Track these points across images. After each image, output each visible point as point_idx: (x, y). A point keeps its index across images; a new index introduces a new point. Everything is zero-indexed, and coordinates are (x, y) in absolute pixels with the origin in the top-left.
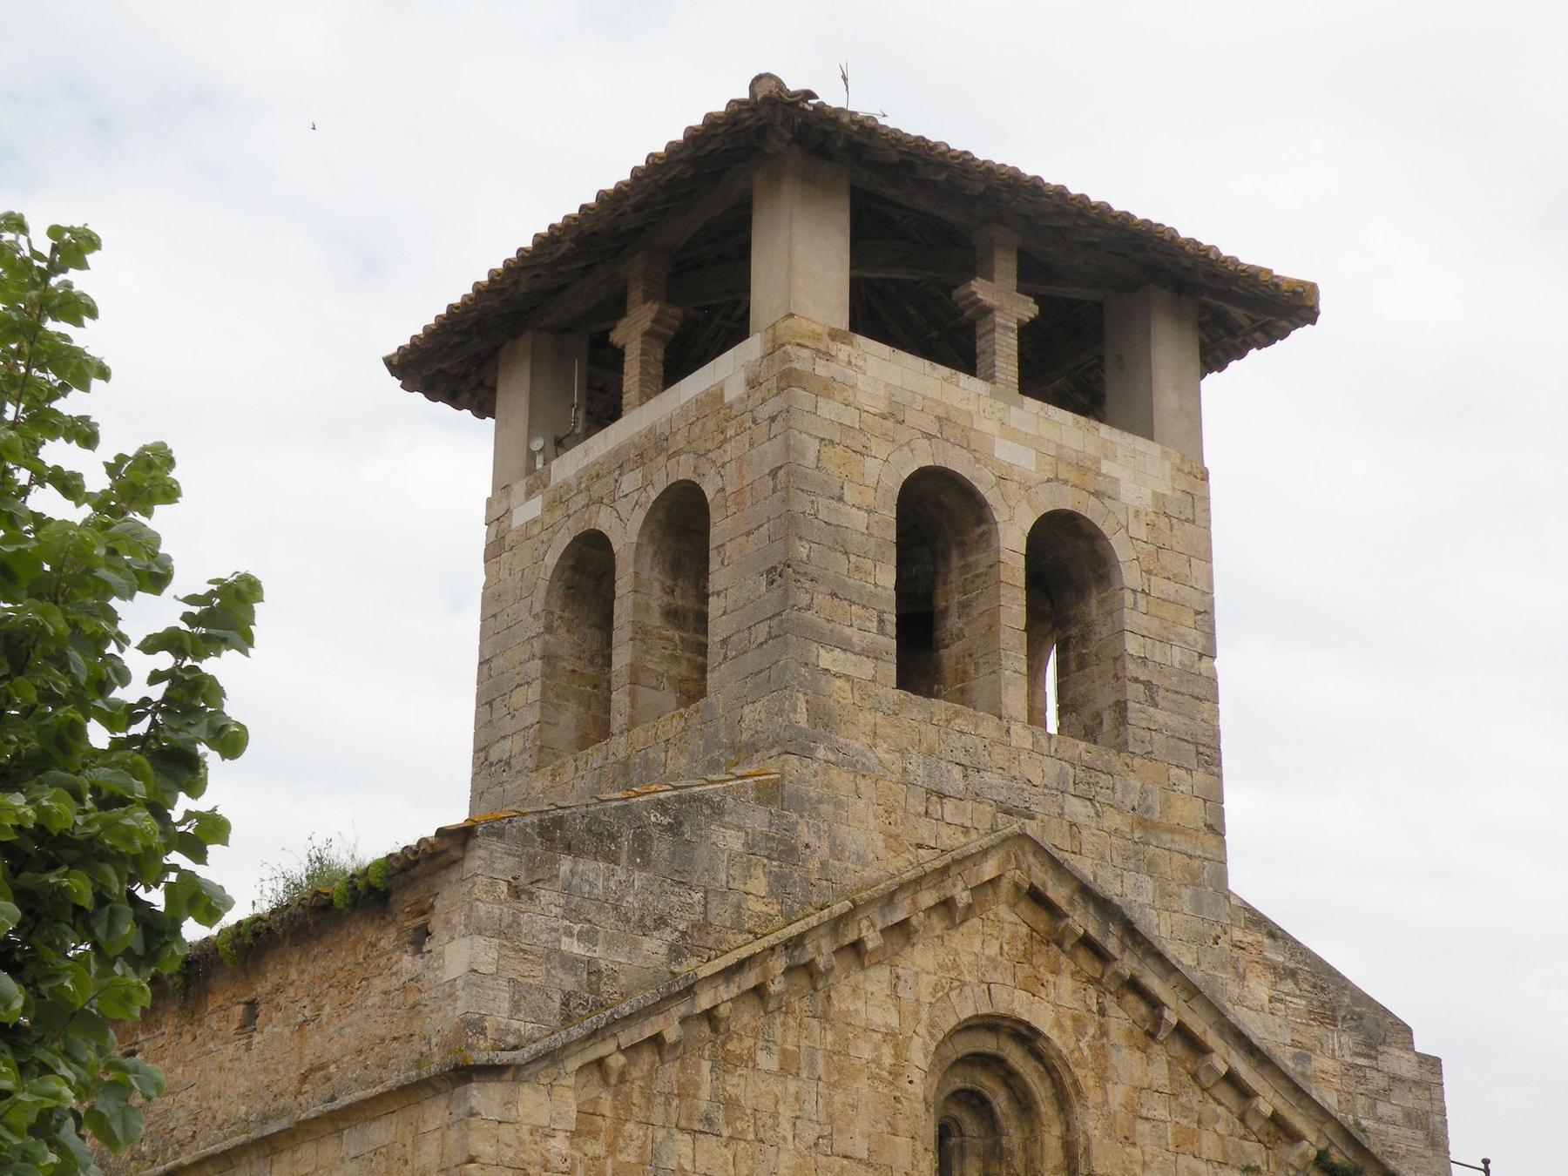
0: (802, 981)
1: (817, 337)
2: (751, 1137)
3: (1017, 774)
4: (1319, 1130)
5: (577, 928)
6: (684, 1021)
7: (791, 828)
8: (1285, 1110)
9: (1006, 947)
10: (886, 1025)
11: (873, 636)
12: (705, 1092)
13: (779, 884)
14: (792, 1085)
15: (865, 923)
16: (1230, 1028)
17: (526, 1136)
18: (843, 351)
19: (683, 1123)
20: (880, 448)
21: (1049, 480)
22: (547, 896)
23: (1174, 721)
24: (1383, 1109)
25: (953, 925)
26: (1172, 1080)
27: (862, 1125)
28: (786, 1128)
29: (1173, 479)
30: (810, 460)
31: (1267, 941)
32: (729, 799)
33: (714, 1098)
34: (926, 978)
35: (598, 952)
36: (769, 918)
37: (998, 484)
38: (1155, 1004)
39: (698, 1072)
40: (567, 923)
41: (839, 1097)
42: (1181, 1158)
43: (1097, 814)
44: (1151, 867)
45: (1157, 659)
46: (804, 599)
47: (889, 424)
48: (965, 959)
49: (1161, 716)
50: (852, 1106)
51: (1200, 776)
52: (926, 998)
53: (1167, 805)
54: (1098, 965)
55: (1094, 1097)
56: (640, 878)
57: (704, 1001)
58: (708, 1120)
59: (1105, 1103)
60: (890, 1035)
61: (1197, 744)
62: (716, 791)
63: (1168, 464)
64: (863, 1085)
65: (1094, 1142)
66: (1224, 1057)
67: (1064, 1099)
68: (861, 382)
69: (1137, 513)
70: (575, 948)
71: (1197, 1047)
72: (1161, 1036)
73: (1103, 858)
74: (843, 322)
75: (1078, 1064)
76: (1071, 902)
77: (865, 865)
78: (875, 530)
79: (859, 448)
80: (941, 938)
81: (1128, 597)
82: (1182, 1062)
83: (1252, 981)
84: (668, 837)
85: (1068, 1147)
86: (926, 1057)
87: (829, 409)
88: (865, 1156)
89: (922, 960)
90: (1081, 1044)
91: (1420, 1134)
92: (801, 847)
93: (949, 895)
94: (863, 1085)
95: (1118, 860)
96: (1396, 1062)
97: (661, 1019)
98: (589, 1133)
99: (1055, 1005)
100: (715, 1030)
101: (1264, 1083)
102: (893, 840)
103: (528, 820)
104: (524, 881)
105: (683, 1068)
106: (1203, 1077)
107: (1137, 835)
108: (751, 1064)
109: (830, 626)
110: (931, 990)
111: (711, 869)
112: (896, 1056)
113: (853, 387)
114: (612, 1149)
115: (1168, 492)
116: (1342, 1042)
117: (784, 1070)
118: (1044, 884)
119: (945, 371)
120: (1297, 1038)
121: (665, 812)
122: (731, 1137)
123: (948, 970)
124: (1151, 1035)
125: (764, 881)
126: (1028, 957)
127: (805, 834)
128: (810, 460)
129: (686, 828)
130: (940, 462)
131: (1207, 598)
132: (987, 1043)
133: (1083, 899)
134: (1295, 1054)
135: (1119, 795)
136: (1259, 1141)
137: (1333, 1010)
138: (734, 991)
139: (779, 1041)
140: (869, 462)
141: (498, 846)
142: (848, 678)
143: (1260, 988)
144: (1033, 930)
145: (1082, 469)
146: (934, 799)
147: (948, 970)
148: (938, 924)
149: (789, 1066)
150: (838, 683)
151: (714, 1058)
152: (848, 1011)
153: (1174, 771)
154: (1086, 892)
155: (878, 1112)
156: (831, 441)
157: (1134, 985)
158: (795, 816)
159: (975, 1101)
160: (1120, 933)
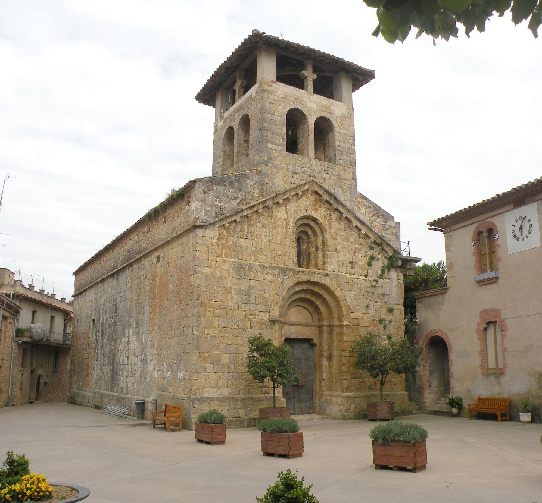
0: (266, 210)
1: (269, 82)
5: (218, 200)
6: (241, 217)
7: (264, 180)
8: (367, 233)
10: (284, 218)
11: (281, 142)
12: (246, 231)
13: (261, 191)
14: (264, 229)
15: (279, 198)
17: (208, 239)
18: (274, 85)
19: (241, 237)
20: (283, 104)
21: (319, 110)
22: (211, 193)
23: (346, 158)
24: (387, 232)
25: (299, 199)
26: (345, 228)
28: (263, 238)
29: (346, 110)
30: (267, 107)
31: (365, 201)
32: (250, 174)
33: (248, 232)
35: (222, 204)
36: (259, 197)
37: (308, 111)
38: (341, 213)
39: (244, 226)
40: (216, 199)
43: (329, 176)
44: (341, 187)
45: (343, 146)
46: (266, 134)
47: (285, 99)
48: (301, 205)
49: (343, 157)
50: (277, 233)
51: (351, 169)
52: (293, 213)
53: (344, 175)
54: (329, 206)
55: (328, 231)
56: (231, 190)
57: (245, 214)
58: (247, 236)
59: (331, 232)
60: (285, 220)
61: (351, 163)
62: (247, 173)
63: (345, 107)
64: (280, 229)
65: (328, 239)
66: (355, 223)
67: (322, 232)
68: (278, 91)
69: (338, 117)
70: (218, 204)
71: (350, 221)
72: (342, 219)
73: (330, 185)
74: (275, 80)
75: (325, 225)
76: (323, 194)
77: (279, 187)
78: (281, 120)
79: (278, 104)
80: (296, 201)
81: (336, 134)
82: (347, 224)
83: (361, 209)
84: (237, 182)
85: (323, 241)
86: (293, 224)
87: (271, 97)
89: (292, 206)
91: (395, 237)
92: (266, 184)
94: (280, 229)
95: (333, 185)
96: (391, 223)
98: (222, 239)
99: (320, 214)
100: (248, 219)
102: (285, 182)
103: (207, 179)
104: (206, 191)
105: (241, 226)
107: (338, 181)
109: (272, 140)
111: (246, 188)
112: (286, 224)
113: (277, 92)
114: (227, 241)
115: (345, 113)
116: (380, 220)
118: (318, 190)
119: (297, 89)
120: (370, 219)
121: (236, 177)
122: (252, 239)
124: (340, 219)
125: (258, 190)
126: (315, 204)
127: (266, 181)
128: (267, 107)
129: (241, 180)
130: (296, 107)
131: (353, 134)
132: (307, 222)
134: (370, 222)
135: (334, 173)
137: (378, 214)
138: (251, 211)
140: (280, 107)
141: (201, 184)
142: (276, 150)
143: (363, 210)
145: (326, 108)
146: (294, 174)
148: (295, 198)
149: (264, 226)
150: (274, 151)
151: (248, 224)
153: (346, 168)
154: (326, 192)
155: (282, 234)
156: (272, 103)
157: (337, 210)
158: (264, 177)
159: (305, 233)
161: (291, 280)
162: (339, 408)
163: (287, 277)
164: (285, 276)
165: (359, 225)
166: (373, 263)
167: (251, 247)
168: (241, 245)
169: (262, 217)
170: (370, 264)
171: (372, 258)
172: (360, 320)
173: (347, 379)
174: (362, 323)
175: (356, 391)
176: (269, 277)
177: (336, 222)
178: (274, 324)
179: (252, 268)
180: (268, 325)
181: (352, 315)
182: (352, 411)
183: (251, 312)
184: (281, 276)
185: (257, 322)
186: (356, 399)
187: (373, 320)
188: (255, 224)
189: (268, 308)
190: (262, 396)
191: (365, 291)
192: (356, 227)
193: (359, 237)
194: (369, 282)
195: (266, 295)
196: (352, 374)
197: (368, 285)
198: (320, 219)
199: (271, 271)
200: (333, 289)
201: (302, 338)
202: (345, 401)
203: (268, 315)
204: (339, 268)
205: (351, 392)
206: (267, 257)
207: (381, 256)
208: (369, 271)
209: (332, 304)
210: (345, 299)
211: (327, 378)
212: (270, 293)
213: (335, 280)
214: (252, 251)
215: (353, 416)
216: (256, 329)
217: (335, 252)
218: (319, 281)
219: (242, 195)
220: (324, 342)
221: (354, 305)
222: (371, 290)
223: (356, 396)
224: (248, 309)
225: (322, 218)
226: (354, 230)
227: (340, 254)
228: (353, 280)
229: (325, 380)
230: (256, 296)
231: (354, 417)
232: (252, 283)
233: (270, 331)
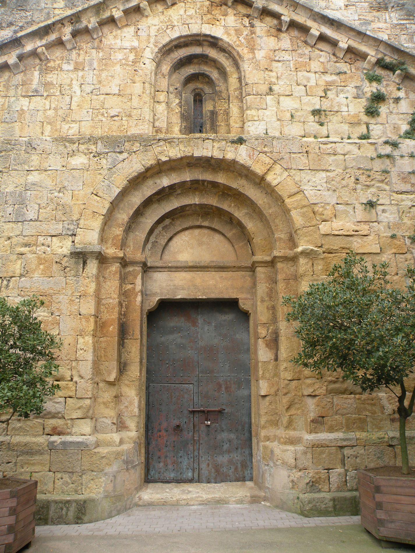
2: (58, 93)
4: (377, 50)
9: (197, 11)
12: (36, 81)
14: (80, 73)
15: (114, 10)
16: (317, 15)
19: (24, 94)
26: (292, 45)
27: (117, 81)
28: (76, 88)
34: (154, 27)
38: (277, 16)
39: (33, 75)
41: (104, 75)
42: (299, 73)
50: (112, 76)
52: (153, 32)
57: (29, 47)
58: (36, 91)
60: (133, 49)
64: (118, 68)
65: (247, 72)
66: (316, 29)
71: (304, 30)
72: (284, 28)
75: (238, 46)
86: (152, 54)
88: (117, 92)
90: (240, 39)
97: (6, 57)
99: (224, 26)
101: (342, 36)
106: (309, 41)
108: (59, 69)
110: (156, 30)
112: (136, 56)
117: (76, 69)
122: (48, 96)
123: (166, 23)
124: (279, 30)
136: (346, 62)
138: (44, 42)
139: (74, 59)
144: (212, 2)
147: (166, 23)
151: (40, 70)
152: (111, 44)
155: (124, 76)
161: (134, 160)
162: (289, 476)
163: (125, 155)
164: (121, 152)
165: (329, 32)
166: (383, 109)
167: (45, 110)
168: (22, 110)
169: (74, 52)
170: (371, 112)
171: (379, 98)
172: (351, 239)
173: (315, 396)
174: (357, 245)
175: (349, 427)
176: (79, 161)
178: (85, 263)
179: (36, 146)
180: (67, 264)
181: (324, 228)
182: (334, 487)
183: (26, 238)
184: (109, 154)
185: (39, 258)
186: (347, 452)
187: (393, 237)
188: (59, 67)
189: (69, 227)
190: (42, 440)
191: (359, 169)
192: (322, 38)
193: (335, 60)
194: (373, 148)
195: (66, 198)
196: (335, 382)
197: (369, 155)
198: (225, 38)
199: (82, 147)
200: (259, 169)
201: (204, 297)
202: (309, 456)
203: (70, 243)
204: (282, 125)
205: (331, 430)
206: (83, 123)
207: (406, 92)
208: (371, 128)
209: (270, 208)
210: (296, 190)
211: (272, 391)
212: (76, 192)
213: (266, 149)
214: (46, 117)
215: (331, 504)
216: (36, 275)
217: (267, 94)
218: (217, 154)
219: (27, 17)
220: (259, 303)
221: (328, 204)
222: (378, 165)
223: (345, 443)
224: (19, 233)
225: (229, 34)
226: (318, 46)
227: (282, 98)
228: (321, 146)
229: (268, 398)
230: (39, 202)
231: (334, 507)
232: (33, 177)
233: (71, 280)
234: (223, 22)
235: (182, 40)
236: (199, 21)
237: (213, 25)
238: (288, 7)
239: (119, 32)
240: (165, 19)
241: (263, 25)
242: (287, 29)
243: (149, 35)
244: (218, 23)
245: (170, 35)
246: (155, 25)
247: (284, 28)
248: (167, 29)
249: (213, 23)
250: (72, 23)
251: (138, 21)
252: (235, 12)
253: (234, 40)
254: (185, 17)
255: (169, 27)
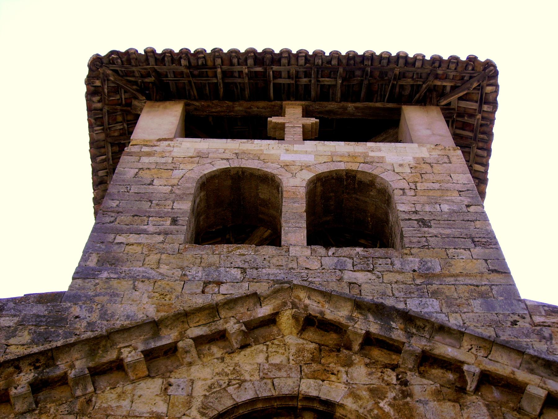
3: (295, 266)
9: (291, 358)
16: (536, 362)
49: (433, 231)
52: (199, 390)
72: (471, 385)
90: (381, 405)
93: (221, 328)
99: (347, 383)
110: (207, 387)
118: (322, 313)
123: (227, 375)
133: (361, 313)
160: (402, 326)
177: (439, 400)
234: (344, 376)
235: (260, 406)
236: (295, 375)
237: (323, 381)
238: (473, 350)
239: (129, 387)
240: (226, 370)
241: (425, 381)
242: (477, 389)
243: (190, 395)
244: (333, 378)
245: (234, 396)
246: (205, 380)
247: (471, 385)
248: (229, 385)
249: (324, 377)
250: (36, 368)
251: (171, 372)
252: (368, 361)
253: (369, 408)
254: (267, 366)
255: (234, 382)
